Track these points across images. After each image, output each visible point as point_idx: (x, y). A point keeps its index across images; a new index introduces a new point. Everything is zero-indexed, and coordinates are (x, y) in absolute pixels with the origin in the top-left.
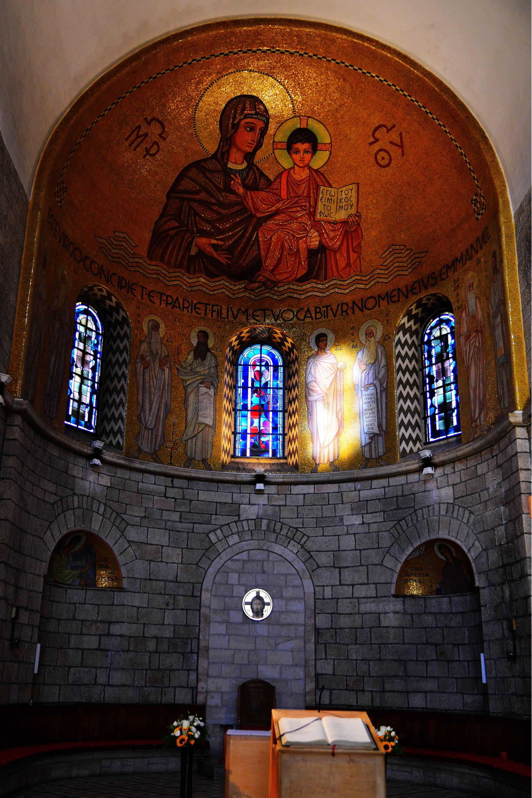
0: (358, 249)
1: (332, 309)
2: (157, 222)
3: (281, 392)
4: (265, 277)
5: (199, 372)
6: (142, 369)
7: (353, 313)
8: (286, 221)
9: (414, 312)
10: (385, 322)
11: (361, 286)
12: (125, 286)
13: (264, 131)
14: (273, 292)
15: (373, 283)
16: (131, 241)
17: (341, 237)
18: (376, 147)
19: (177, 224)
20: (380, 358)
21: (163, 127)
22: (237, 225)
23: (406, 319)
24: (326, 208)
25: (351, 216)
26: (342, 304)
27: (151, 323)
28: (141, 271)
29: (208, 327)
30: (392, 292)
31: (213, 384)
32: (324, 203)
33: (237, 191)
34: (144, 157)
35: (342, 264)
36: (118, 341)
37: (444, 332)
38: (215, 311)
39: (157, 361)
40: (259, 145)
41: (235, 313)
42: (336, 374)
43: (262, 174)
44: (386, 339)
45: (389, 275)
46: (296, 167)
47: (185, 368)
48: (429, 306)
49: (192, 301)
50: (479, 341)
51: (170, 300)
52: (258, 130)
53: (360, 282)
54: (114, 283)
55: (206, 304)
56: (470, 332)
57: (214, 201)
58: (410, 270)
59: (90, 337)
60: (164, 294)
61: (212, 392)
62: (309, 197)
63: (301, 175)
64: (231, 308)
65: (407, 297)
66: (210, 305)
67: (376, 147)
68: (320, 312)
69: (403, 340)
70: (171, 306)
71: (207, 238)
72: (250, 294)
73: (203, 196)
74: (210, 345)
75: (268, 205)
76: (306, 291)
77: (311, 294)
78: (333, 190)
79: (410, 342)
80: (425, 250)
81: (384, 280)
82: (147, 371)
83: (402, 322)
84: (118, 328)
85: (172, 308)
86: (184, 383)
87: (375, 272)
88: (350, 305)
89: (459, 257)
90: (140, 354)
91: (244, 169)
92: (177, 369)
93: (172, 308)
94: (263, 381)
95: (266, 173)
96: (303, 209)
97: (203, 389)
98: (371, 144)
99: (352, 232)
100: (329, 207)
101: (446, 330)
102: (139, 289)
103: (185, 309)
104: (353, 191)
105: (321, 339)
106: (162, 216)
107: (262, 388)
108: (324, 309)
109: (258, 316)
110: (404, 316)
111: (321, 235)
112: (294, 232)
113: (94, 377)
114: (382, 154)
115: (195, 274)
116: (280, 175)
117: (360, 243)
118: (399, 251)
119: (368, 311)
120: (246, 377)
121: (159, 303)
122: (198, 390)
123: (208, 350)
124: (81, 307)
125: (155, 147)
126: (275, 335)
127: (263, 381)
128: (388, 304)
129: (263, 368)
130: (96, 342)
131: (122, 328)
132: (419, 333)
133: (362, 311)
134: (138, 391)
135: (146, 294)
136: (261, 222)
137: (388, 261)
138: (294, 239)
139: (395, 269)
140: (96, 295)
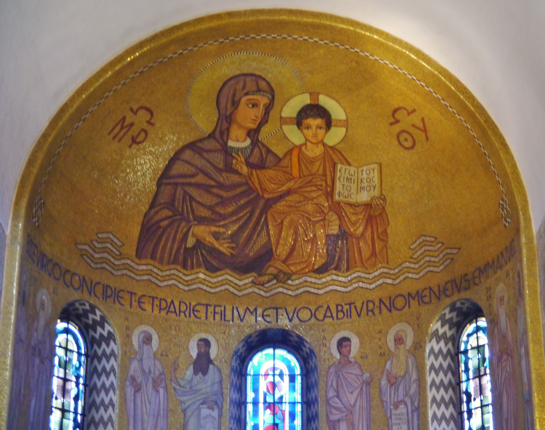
0: (384, 236)
1: (355, 307)
2: (146, 214)
3: (298, 408)
4: (276, 268)
5: (200, 390)
6: (133, 393)
7: (380, 313)
8: (299, 202)
9: (448, 316)
10: (416, 326)
11: (389, 281)
12: (111, 295)
13: (268, 109)
14: (287, 286)
15: (402, 278)
16: (116, 240)
17: (365, 222)
18: (397, 128)
19: (170, 213)
20: (411, 371)
21: (152, 115)
22: (241, 208)
23: (439, 323)
24: (345, 187)
25: (375, 199)
26: (367, 302)
27: (142, 336)
28: (129, 273)
29: (210, 333)
30: (423, 291)
31: (216, 403)
32: (342, 183)
33: (240, 170)
34: (130, 147)
35: (366, 252)
36: (104, 361)
37: (481, 343)
38: (218, 313)
39: (151, 381)
40: (264, 121)
41: (242, 314)
42: (362, 389)
43: (269, 151)
44: (418, 346)
45: (419, 270)
46: (308, 143)
47: (183, 387)
48: (464, 309)
49: (190, 304)
50: (509, 365)
51: (164, 304)
52: (261, 107)
53: (387, 276)
54: (99, 295)
55: (207, 305)
56: (502, 353)
57: (213, 183)
58: (442, 267)
59: (70, 360)
60: (157, 298)
61: (215, 413)
62: (324, 175)
63: (315, 151)
64: (237, 308)
65: (439, 298)
66: (211, 305)
67: (397, 128)
68: (342, 311)
69: (436, 350)
70: (165, 311)
71: (206, 225)
72: (259, 289)
73: (200, 179)
74: (213, 355)
75: (277, 184)
76: (326, 284)
77: (331, 288)
78: (352, 169)
79: (445, 350)
80: (457, 246)
81: (414, 276)
82: (139, 395)
83: (434, 328)
84: (104, 345)
85: (167, 313)
86: (183, 404)
87: (404, 265)
88: (377, 303)
89: (491, 263)
90: (129, 375)
91: (248, 147)
92: (175, 389)
93: (167, 313)
94: (277, 395)
95: (274, 149)
96: (319, 189)
97: (205, 411)
98: (391, 124)
99: (376, 217)
100: (348, 188)
101: (483, 339)
102: (127, 296)
103: (182, 314)
104: (376, 171)
105: (344, 344)
106: (152, 206)
107: (278, 403)
108: (346, 307)
109: (269, 316)
110: (437, 321)
111: (340, 218)
112: (309, 214)
113: (76, 409)
114: (404, 136)
115: (192, 268)
116: (289, 152)
117: (386, 230)
118: (429, 243)
119: (397, 312)
120: (256, 390)
121: (151, 311)
122: (199, 413)
123: (210, 361)
124: (61, 325)
125: (143, 134)
126: (292, 339)
127: (277, 395)
128: (419, 304)
129: (277, 379)
130: (78, 365)
131: (108, 345)
132: (455, 340)
133: (390, 311)
134: (128, 421)
135: (135, 301)
136: (269, 204)
137: (418, 253)
138: (309, 223)
139: (426, 264)
140: (77, 309)
